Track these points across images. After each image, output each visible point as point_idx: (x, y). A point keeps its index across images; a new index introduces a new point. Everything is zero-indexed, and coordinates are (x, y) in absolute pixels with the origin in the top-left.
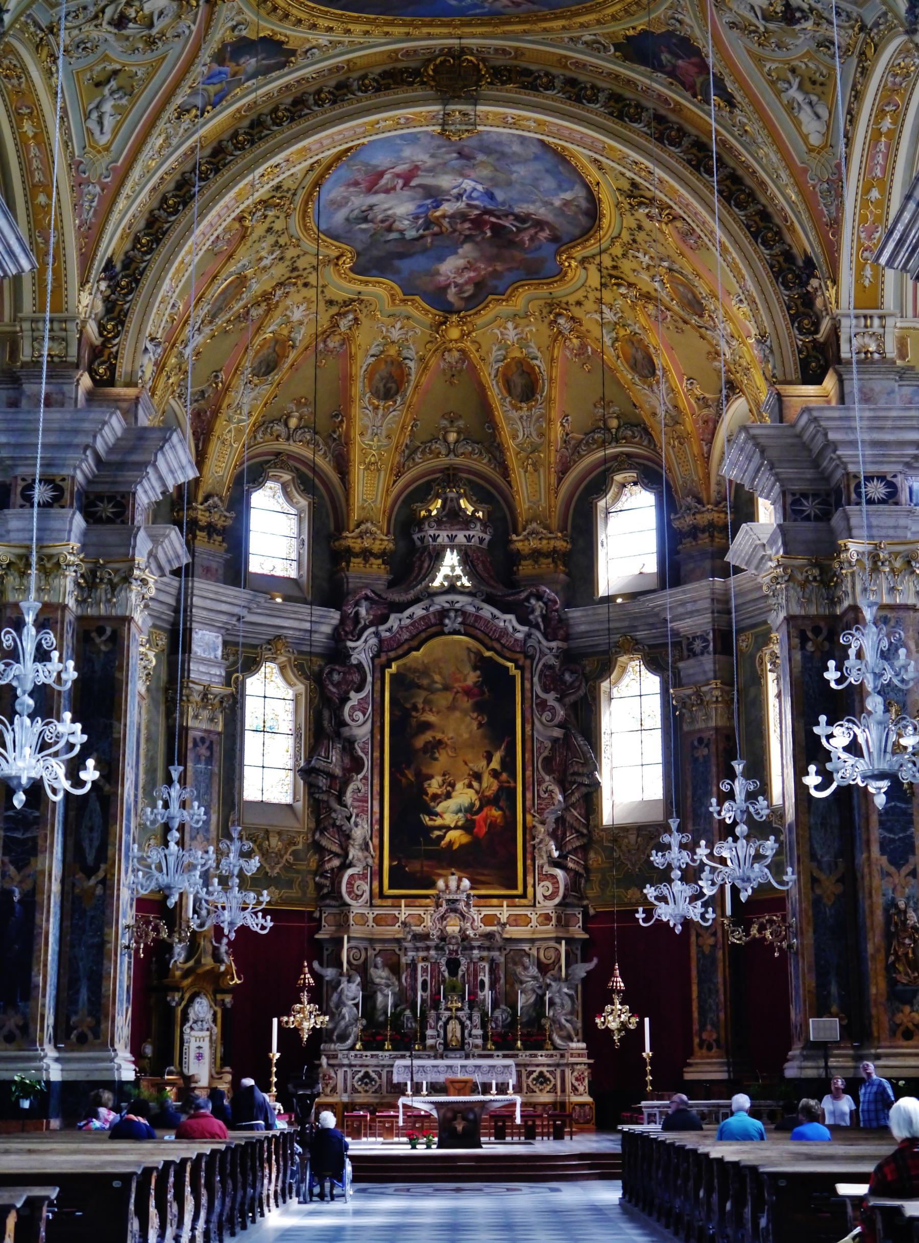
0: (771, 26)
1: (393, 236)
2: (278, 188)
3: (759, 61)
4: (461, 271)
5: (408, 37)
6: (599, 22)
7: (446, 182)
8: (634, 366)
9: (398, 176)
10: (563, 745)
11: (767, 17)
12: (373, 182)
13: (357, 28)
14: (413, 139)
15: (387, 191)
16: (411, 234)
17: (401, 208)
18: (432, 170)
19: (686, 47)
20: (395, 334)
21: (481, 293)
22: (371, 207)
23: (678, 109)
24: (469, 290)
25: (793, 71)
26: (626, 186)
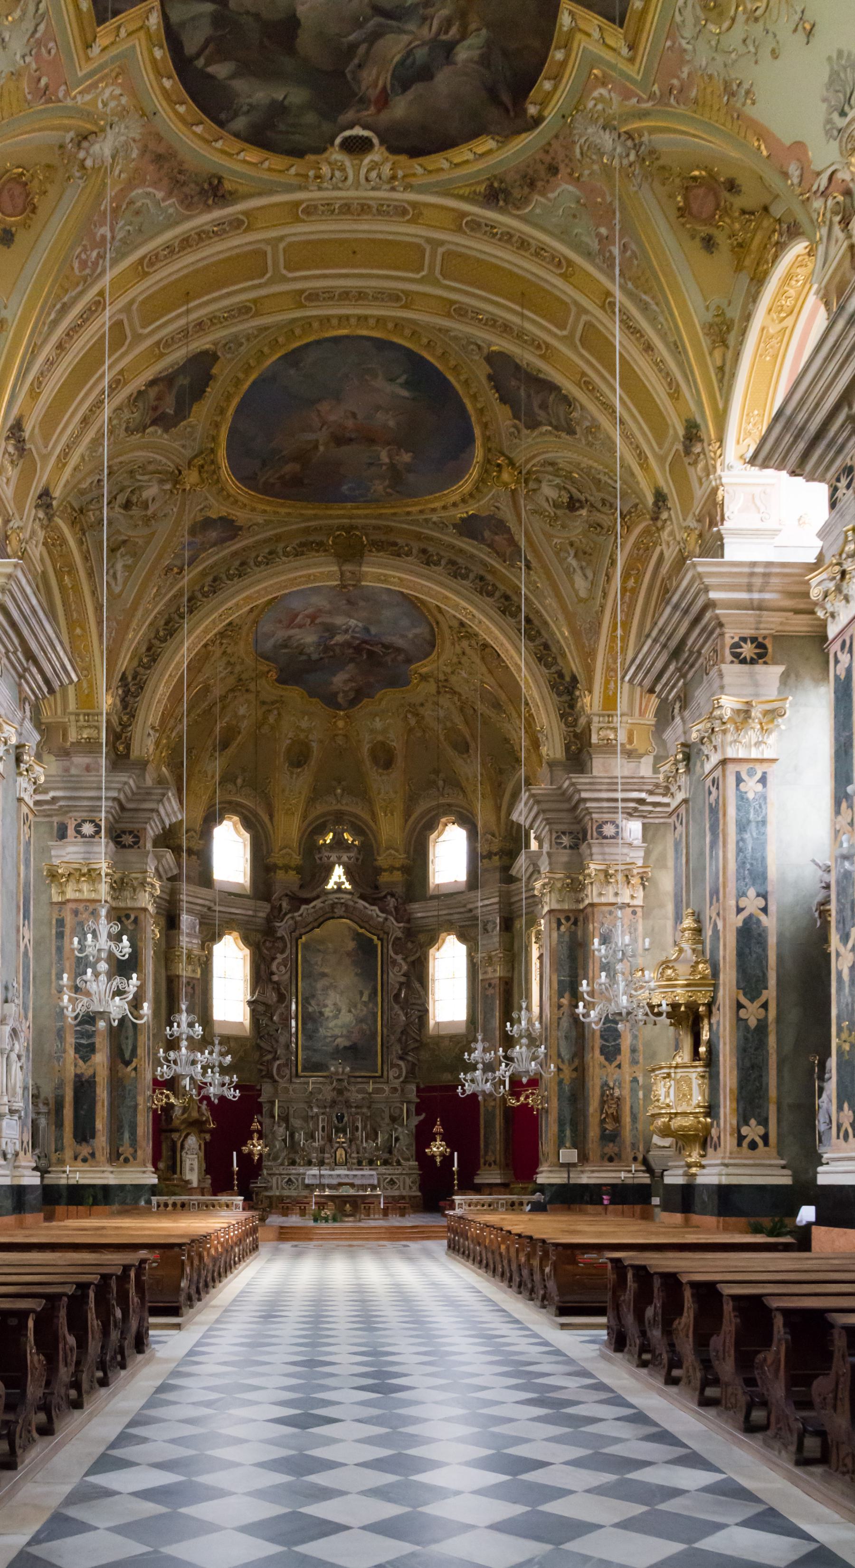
0: (559, 512)
1: (304, 658)
2: (230, 624)
3: (549, 537)
4: (345, 682)
5: (316, 517)
6: (444, 508)
7: (339, 621)
8: (455, 747)
9: (308, 616)
10: (407, 984)
11: (556, 505)
12: (291, 620)
13: (283, 511)
14: (316, 590)
15: (300, 626)
16: (315, 657)
17: (309, 638)
18: (330, 613)
19: (500, 526)
20: (304, 724)
21: (358, 696)
22: (290, 637)
23: (493, 571)
24: (352, 695)
25: (572, 544)
26: (455, 624)
